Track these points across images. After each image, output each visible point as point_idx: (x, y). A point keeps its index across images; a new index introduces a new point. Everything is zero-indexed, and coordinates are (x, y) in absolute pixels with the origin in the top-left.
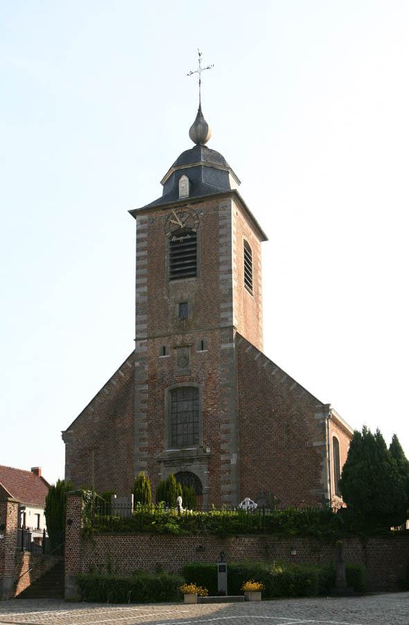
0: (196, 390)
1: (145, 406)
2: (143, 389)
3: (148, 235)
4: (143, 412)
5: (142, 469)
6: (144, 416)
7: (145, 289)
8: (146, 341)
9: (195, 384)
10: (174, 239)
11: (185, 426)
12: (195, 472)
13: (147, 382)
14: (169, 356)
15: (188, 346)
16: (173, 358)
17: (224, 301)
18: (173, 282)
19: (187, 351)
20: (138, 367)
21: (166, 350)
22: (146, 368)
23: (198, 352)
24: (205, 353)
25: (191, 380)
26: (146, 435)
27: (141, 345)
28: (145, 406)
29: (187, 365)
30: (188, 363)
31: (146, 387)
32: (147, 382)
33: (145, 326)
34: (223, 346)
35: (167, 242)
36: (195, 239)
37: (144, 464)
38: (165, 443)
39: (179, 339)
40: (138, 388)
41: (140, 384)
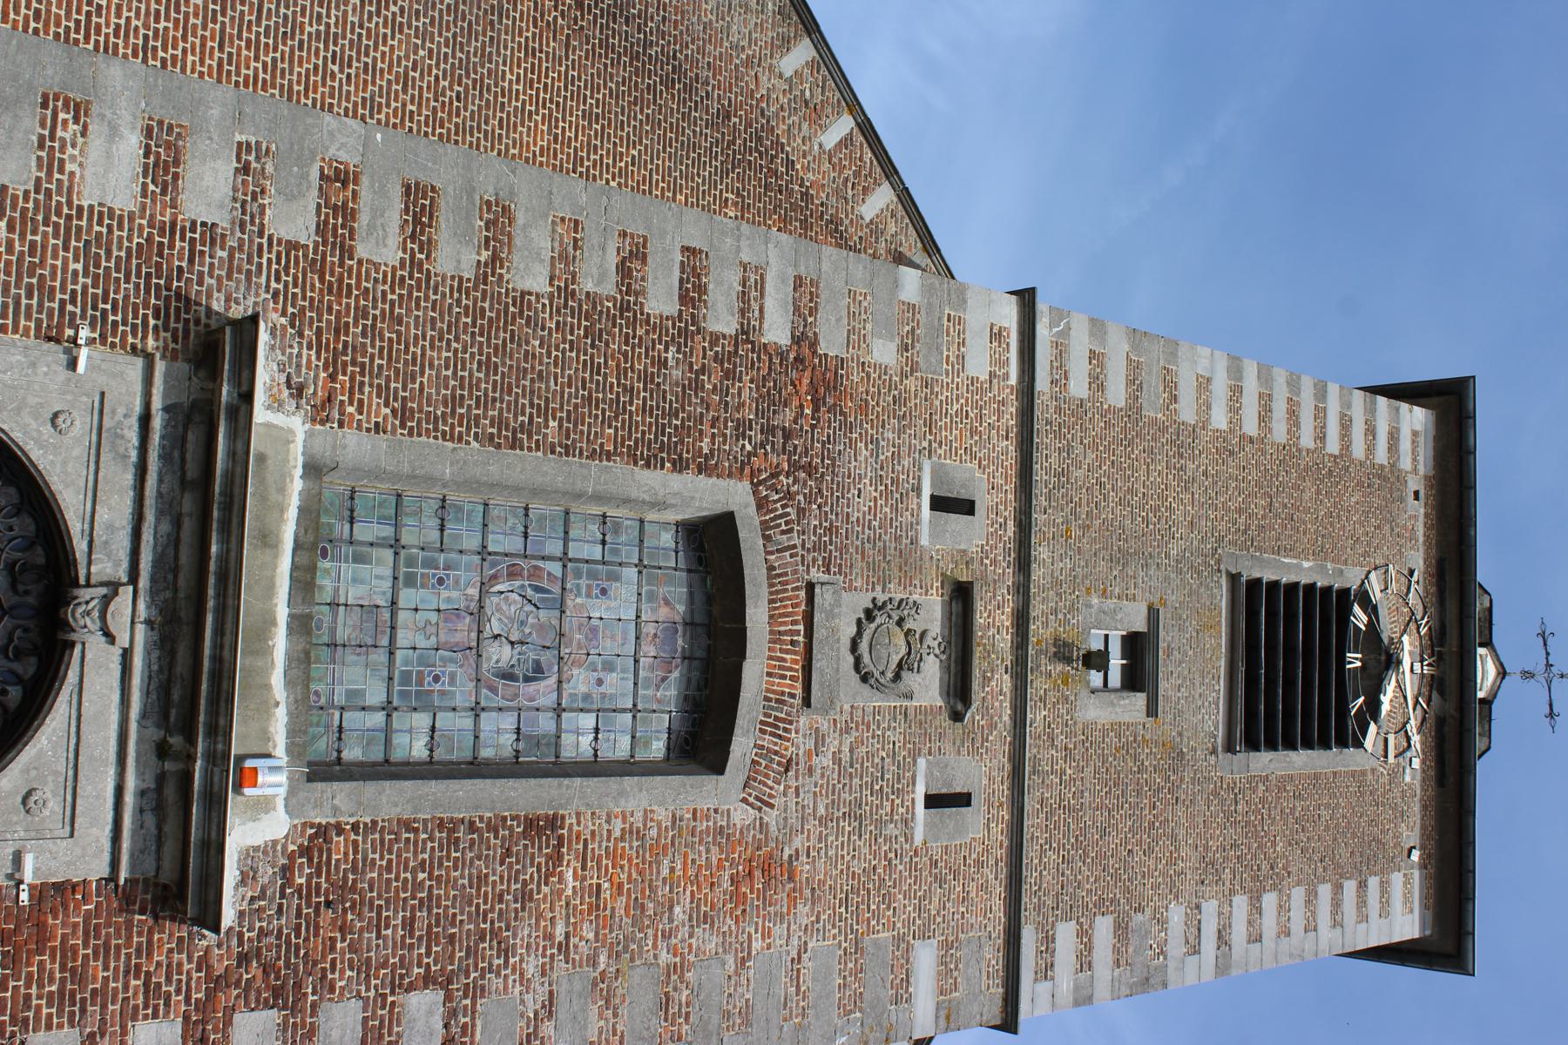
0: (702, 740)
1: (661, 300)
2: (769, 303)
3: (1382, 467)
4: (624, 270)
5: (163, 164)
6: (597, 276)
7: (1219, 419)
8: (1013, 380)
9: (742, 745)
10: (1360, 618)
11: (463, 631)
12: (47, 740)
13: (803, 339)
14: (924, 541)
15: (959, 690)
16: (909, 561)
17: (1122, 930)
18: (1224, 581)
19: (928, 684)
20: (896, 284)
21: (956, 521)
22: (884, 352)
23: (922, 762)
24: (907, 822)
25: (775, 726)
26: (456, 256)
27: (997, 335)
28: (661, 300)
29: (865, 679)
30: (879, 687)
31: (777, 331)
32: (803, 339)
33: (1078, 387)
34: (925, 957)
35: (1351, 579)
36: (1342, 743)
37: (207, 192)
38: (355, 446)
39: (993, 620)
40: (779, 255)
41: (799, 282)
